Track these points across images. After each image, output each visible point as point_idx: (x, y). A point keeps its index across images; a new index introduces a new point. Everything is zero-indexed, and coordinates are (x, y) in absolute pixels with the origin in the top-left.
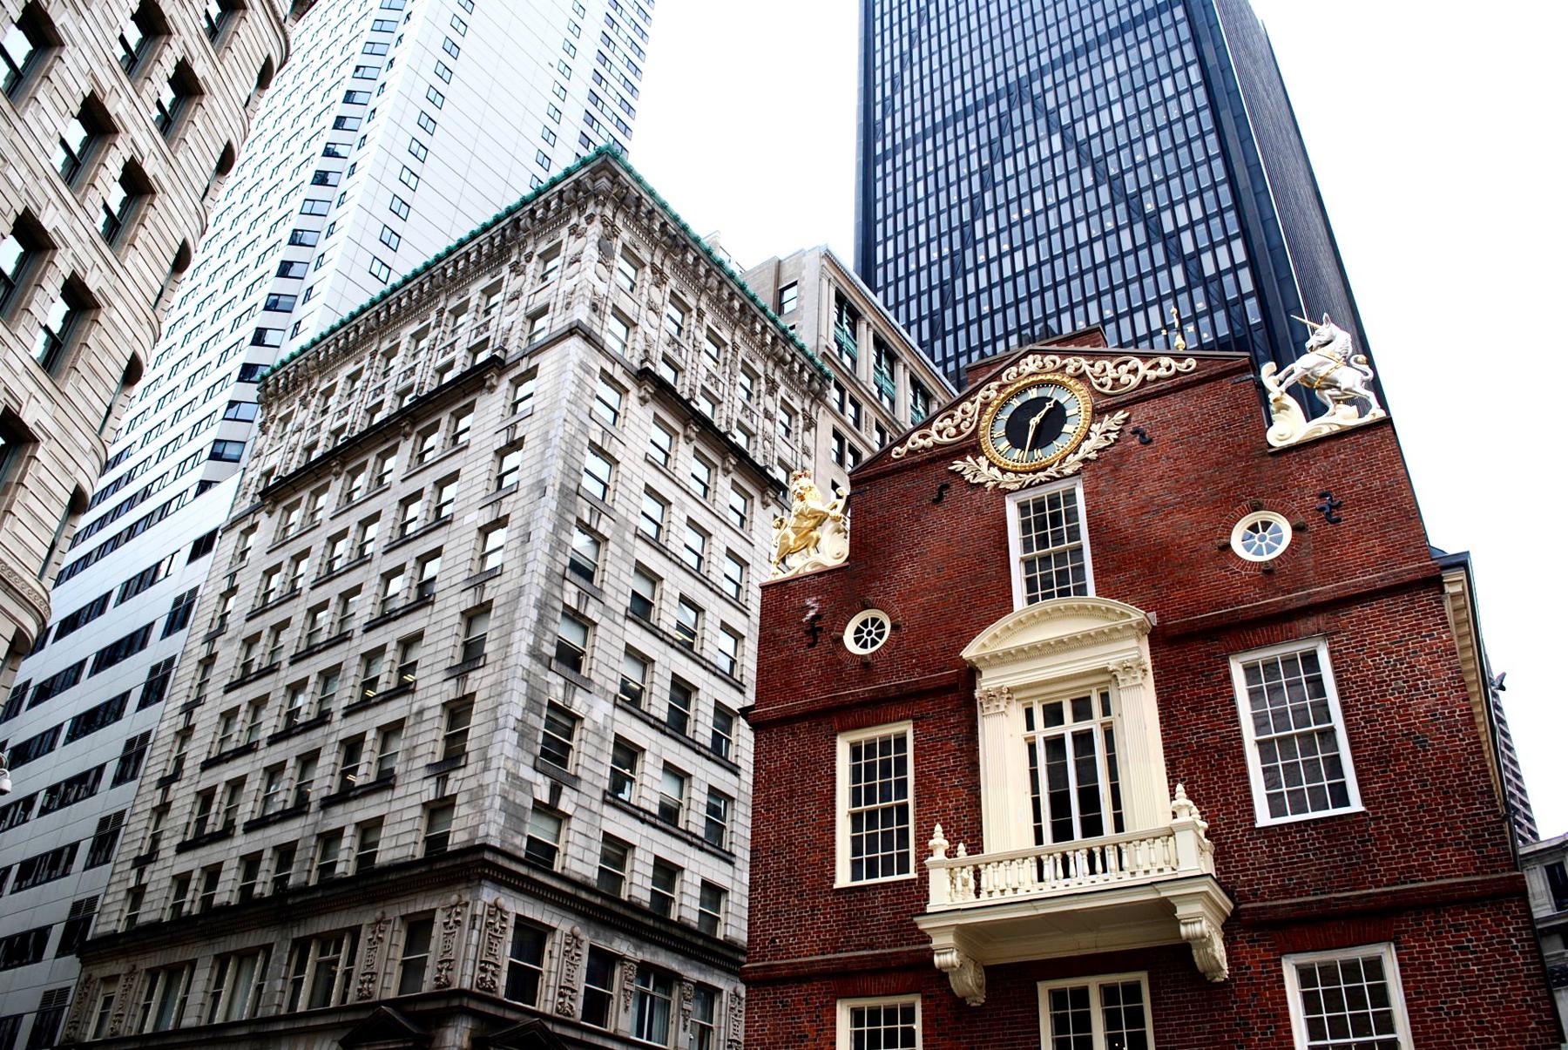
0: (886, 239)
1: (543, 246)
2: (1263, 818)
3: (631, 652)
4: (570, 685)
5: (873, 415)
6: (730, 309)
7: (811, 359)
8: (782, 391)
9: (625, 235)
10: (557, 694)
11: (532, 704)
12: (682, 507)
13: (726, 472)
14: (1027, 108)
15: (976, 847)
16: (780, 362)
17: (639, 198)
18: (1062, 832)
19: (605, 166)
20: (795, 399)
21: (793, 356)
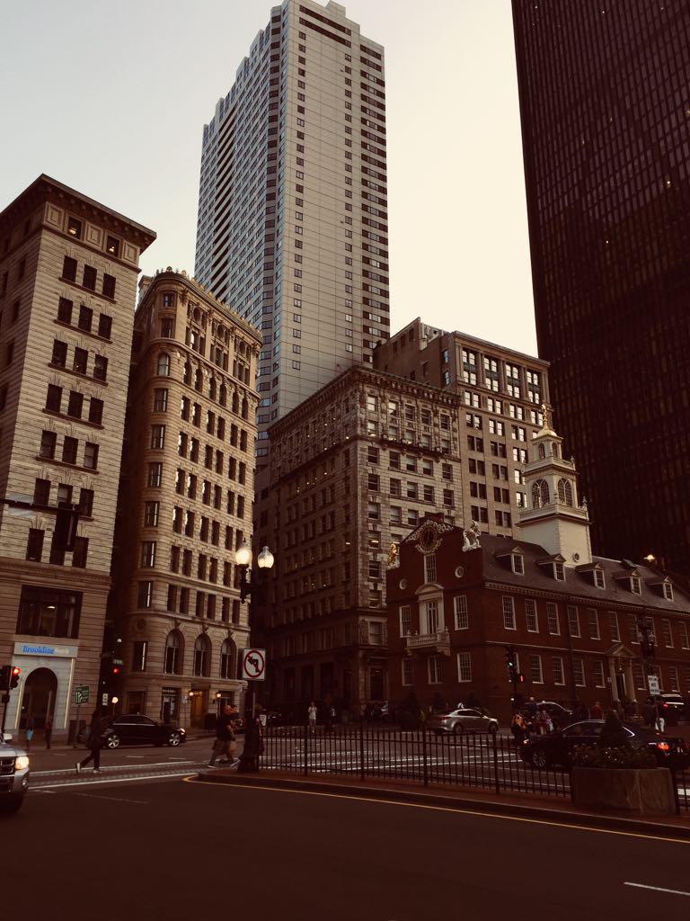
0: (542, 195)
1: (344, 398)
2: (457, 628)
3: (393, 535)
4: (375, 555)
5: (486, 396)
6: (413, 394)
7: (451, 394)
8: (441, 411)
9: (368, 390)
10: (371, 558)
11: (364, 564)
12: (404, 479)
13: (420, 458)
14: (608, 98)
15: (419, 633)
16: (437, 402)
17: (370, 376)
18: (431, 632)
19: (356, 371)
20: (448, 411)
21: (443, 398)
